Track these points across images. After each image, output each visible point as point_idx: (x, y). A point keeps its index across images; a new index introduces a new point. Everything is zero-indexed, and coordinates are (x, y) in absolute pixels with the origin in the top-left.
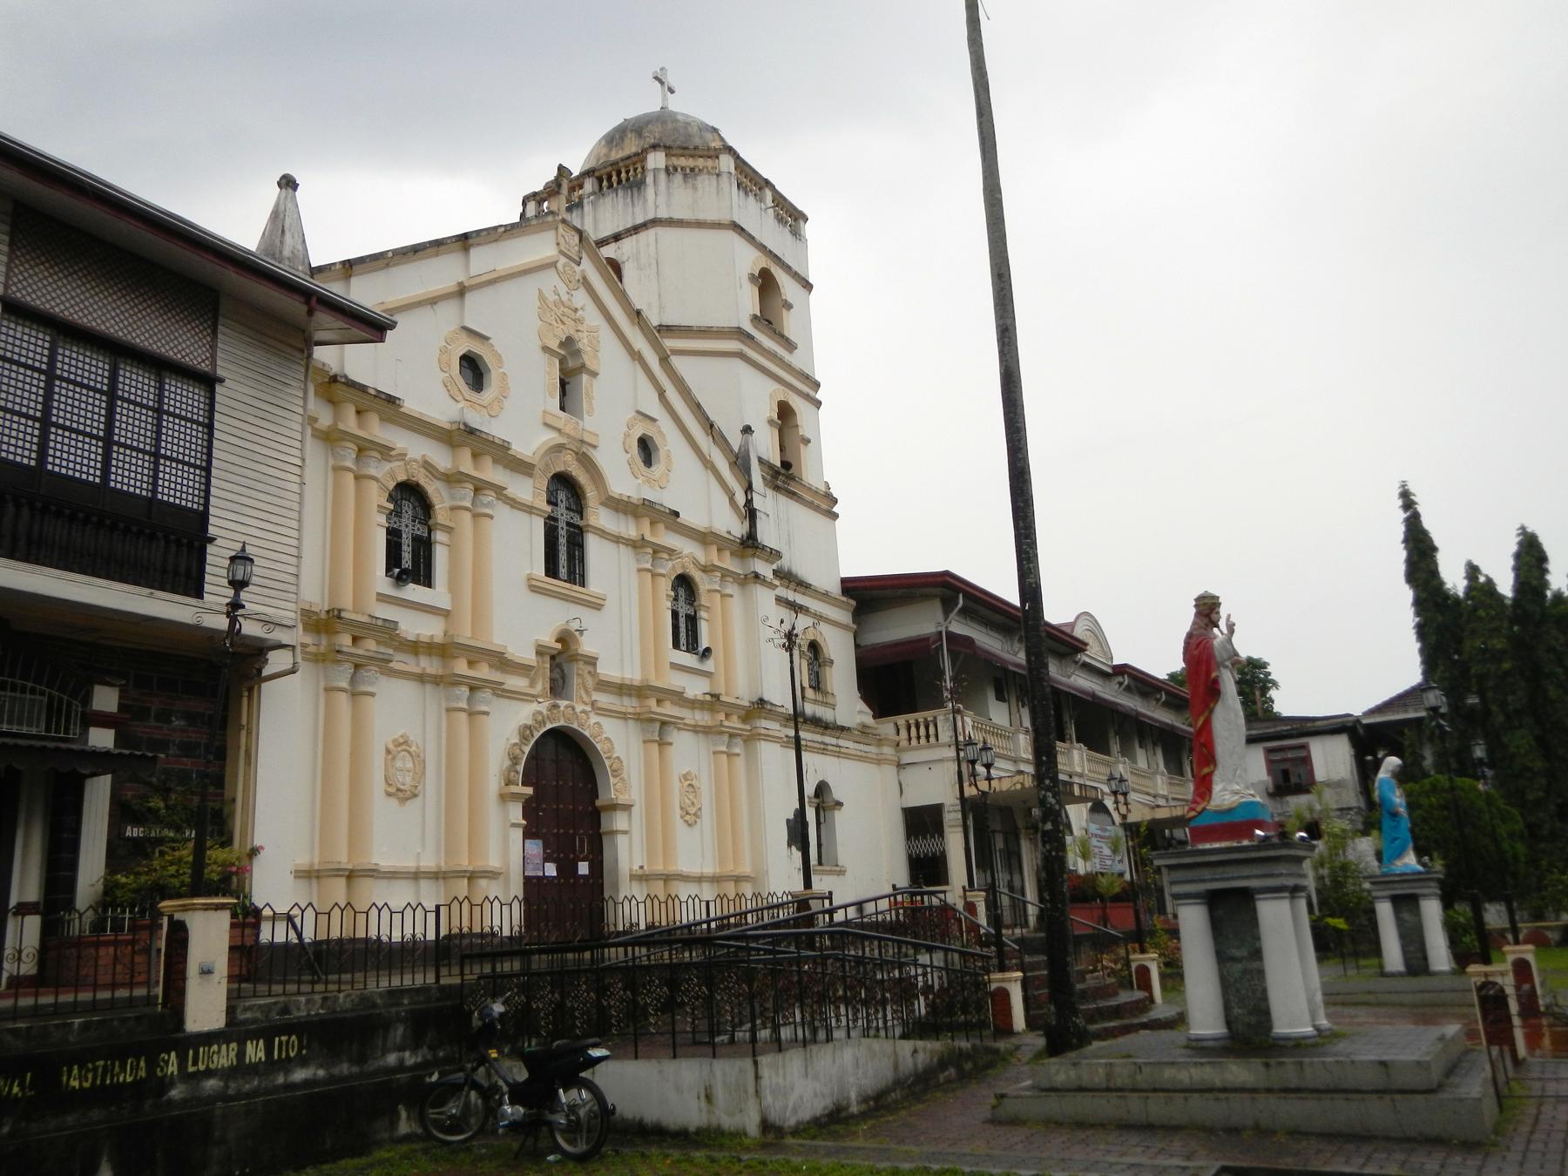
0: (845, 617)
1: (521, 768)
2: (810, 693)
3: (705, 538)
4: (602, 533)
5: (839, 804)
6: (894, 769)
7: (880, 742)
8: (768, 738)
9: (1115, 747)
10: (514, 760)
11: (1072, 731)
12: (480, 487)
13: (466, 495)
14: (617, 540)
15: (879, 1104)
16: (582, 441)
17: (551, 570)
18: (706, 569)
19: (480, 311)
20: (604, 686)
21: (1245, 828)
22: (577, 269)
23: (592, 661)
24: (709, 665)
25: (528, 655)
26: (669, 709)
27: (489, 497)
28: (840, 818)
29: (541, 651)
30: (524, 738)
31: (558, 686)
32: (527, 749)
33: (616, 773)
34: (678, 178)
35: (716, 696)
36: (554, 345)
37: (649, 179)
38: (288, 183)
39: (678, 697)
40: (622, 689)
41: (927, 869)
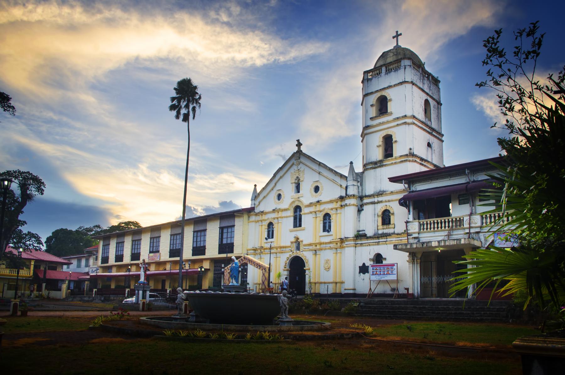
1: (287, 265)
2: (380, 227)
3: (331, 202)
4: (305, 214)
10: (286, 264)
12: (277, 218)
13: (276, 220)
14: (308, 213)
16: (298, 198)
17: (295, 226)
18: (332, 209)
19: (278, 187)
20: (305, 245)
22: (299, 160)
23: (302, 241)
25: (289, 244)
26: (318, 247)
27: (279, 219)
29: (292, 243)
30: (287, 260)
31: (298, 248)
32: (288, 261)
33: (307, 263)
36: (294, 181)
38: (255, 186)
39: (321, 244)
40: (310, 245)
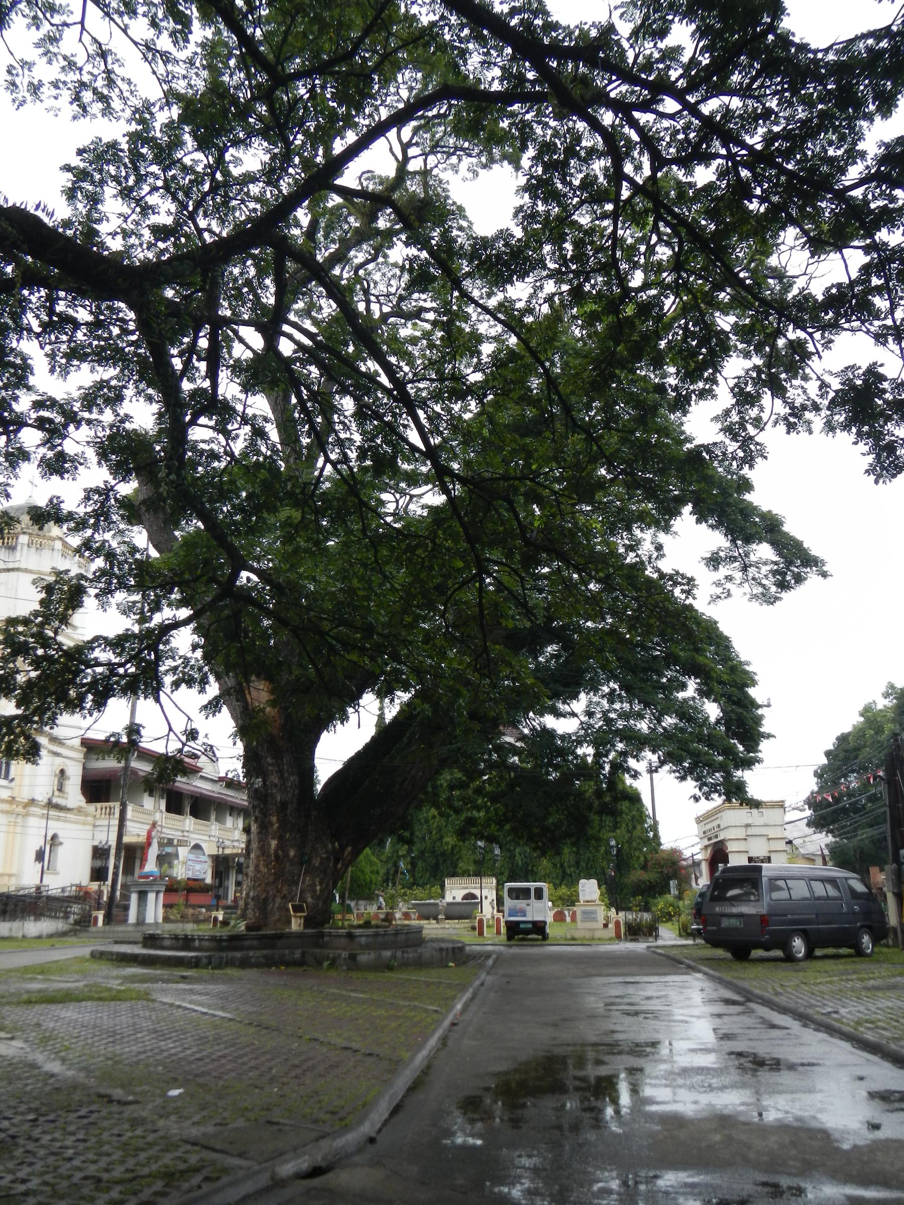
0: (80, 756)
2: (57, 793)
5: (61, 843)
6: (91, 828)
7: (87, 815)
8: (33, 815)
9: (213, 817)
11: (188, 810)
15: (50, 936)
21: (147, 877)
24: (13, 784)
28: (61, 850)
34: (33, 550)
35: (13, 798)
37: (19, 548)
41: (98, 874)
